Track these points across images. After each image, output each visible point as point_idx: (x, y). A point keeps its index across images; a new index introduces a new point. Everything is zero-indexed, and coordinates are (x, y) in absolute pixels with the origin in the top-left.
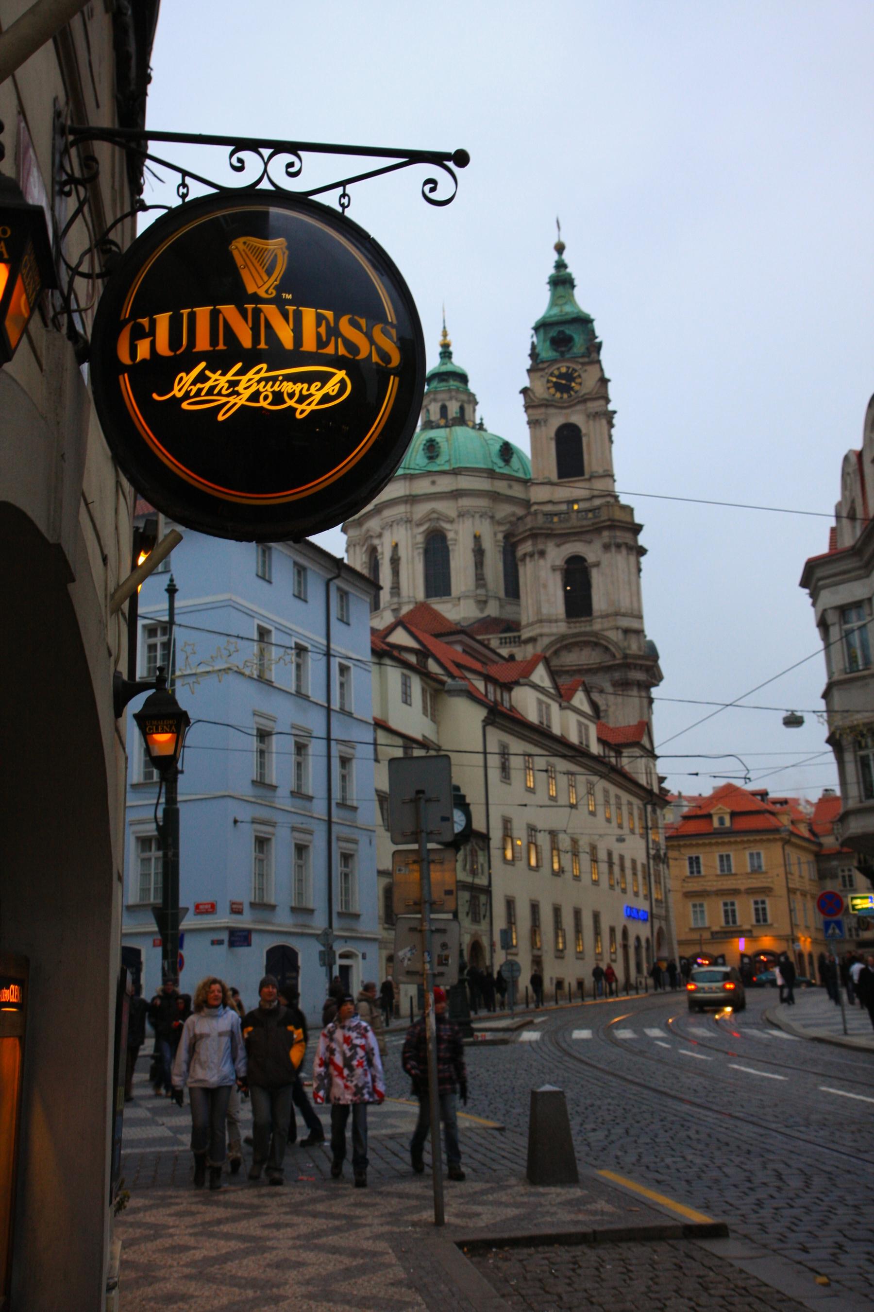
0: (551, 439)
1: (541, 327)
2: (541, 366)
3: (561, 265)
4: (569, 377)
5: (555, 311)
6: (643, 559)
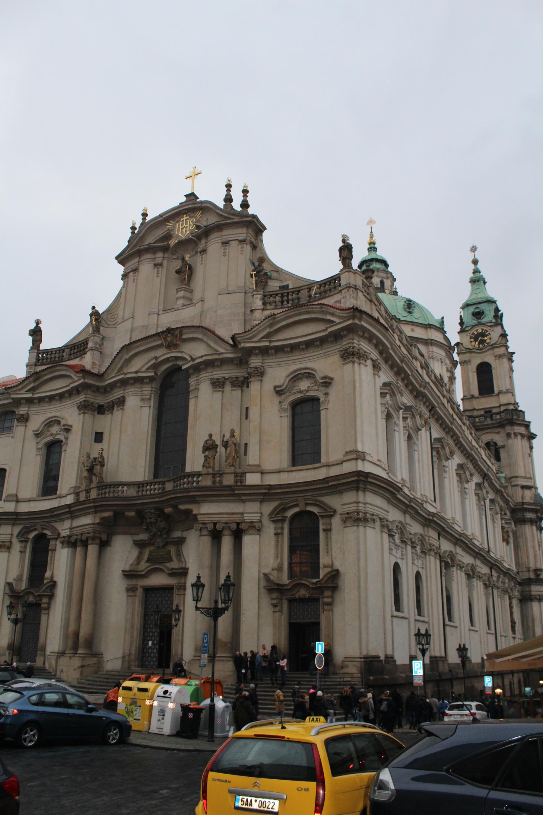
0: (474, 372)
1: (466, 306)
2: (466, 329)
3: (476, 271)
4: (483, 334)
5: (474, 296)
6: (534, 441)
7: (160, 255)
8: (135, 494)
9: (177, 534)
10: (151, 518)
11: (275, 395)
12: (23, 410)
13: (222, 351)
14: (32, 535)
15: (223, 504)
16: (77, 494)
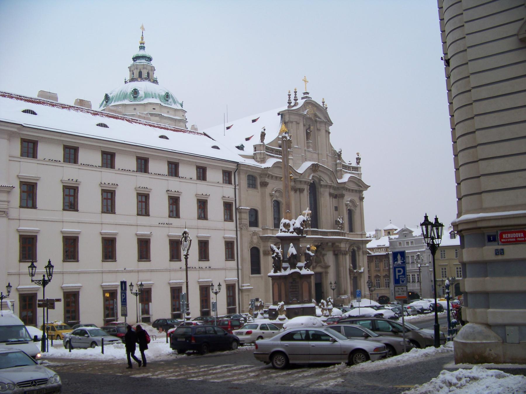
9: (323, 252)
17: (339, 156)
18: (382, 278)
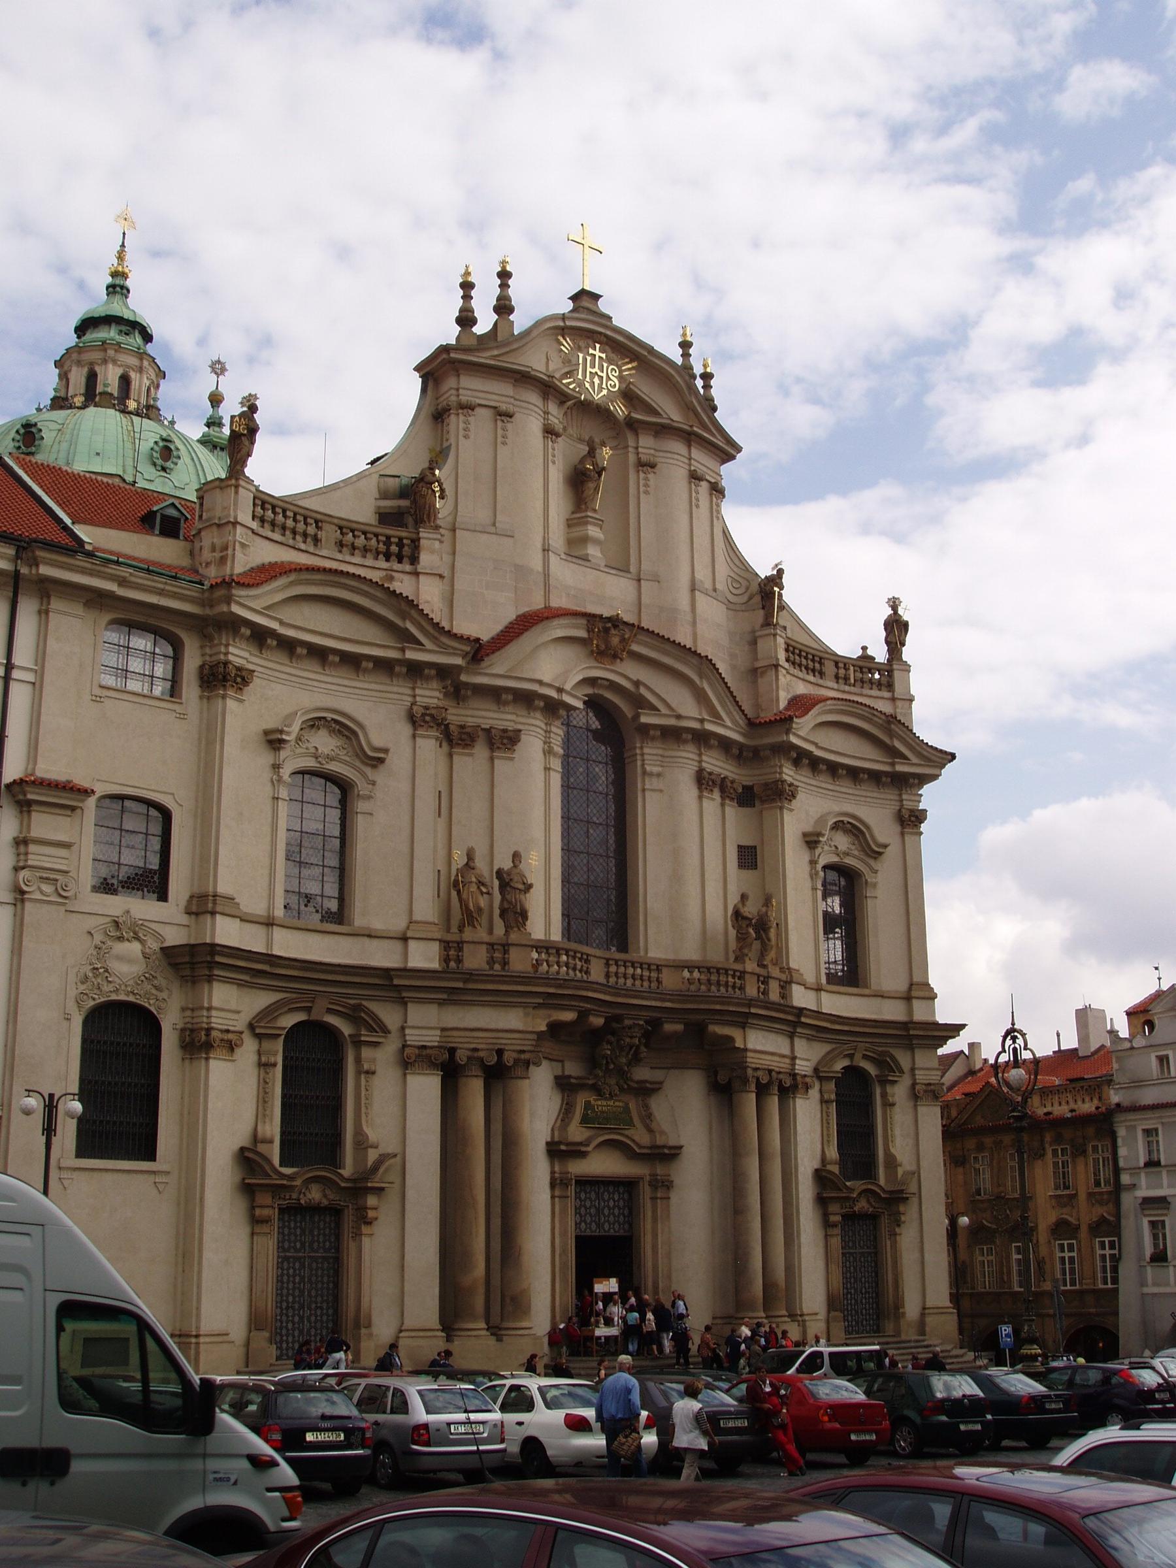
7: (553, 408)
8: (602, 980)
9: (642, 1073)
10: (631, 1037)
11: (804, 846)
12: (239, 654)
13: (729, 724)
14: (288, 1021)
15: (772, 1036)
16: (451, 949)
17: (767, 592)
18: (1084, 1233)
